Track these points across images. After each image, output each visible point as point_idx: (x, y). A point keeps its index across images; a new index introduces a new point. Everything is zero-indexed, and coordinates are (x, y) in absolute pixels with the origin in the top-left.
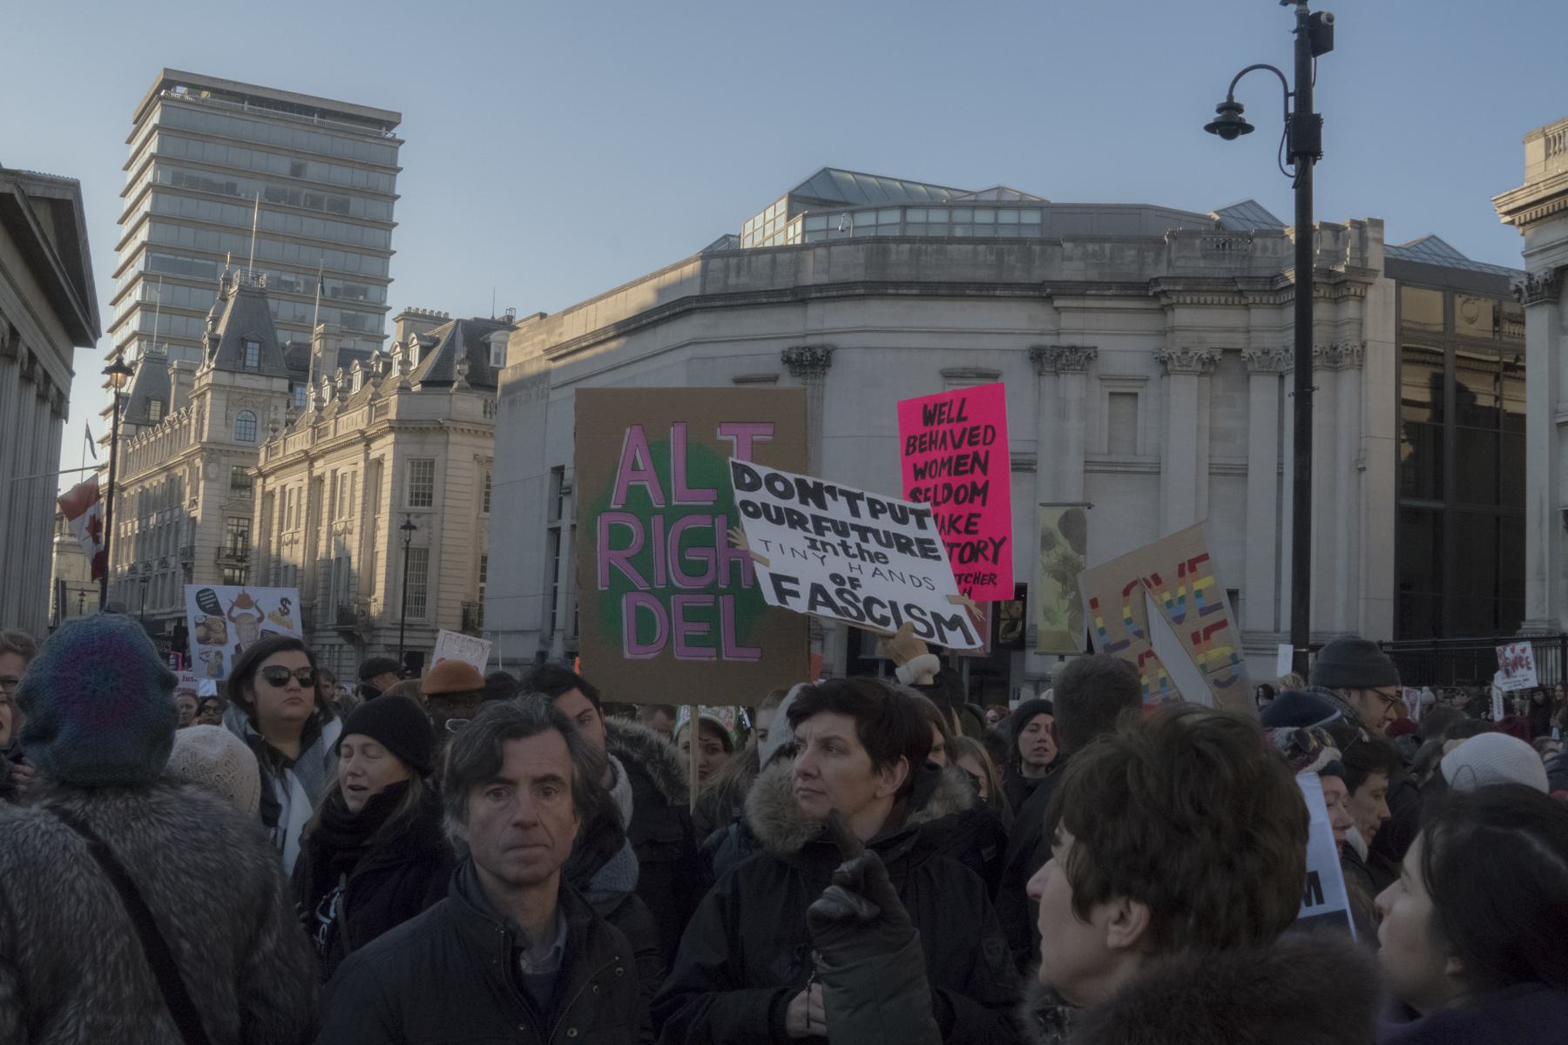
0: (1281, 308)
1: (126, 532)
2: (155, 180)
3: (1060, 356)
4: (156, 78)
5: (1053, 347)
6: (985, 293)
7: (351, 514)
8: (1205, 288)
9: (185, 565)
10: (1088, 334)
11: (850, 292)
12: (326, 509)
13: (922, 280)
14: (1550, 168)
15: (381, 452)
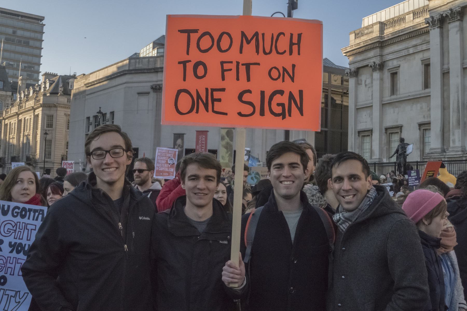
7: (30, 130)
12: (22, 129)
14: (356, 41)
15: (38, 113)
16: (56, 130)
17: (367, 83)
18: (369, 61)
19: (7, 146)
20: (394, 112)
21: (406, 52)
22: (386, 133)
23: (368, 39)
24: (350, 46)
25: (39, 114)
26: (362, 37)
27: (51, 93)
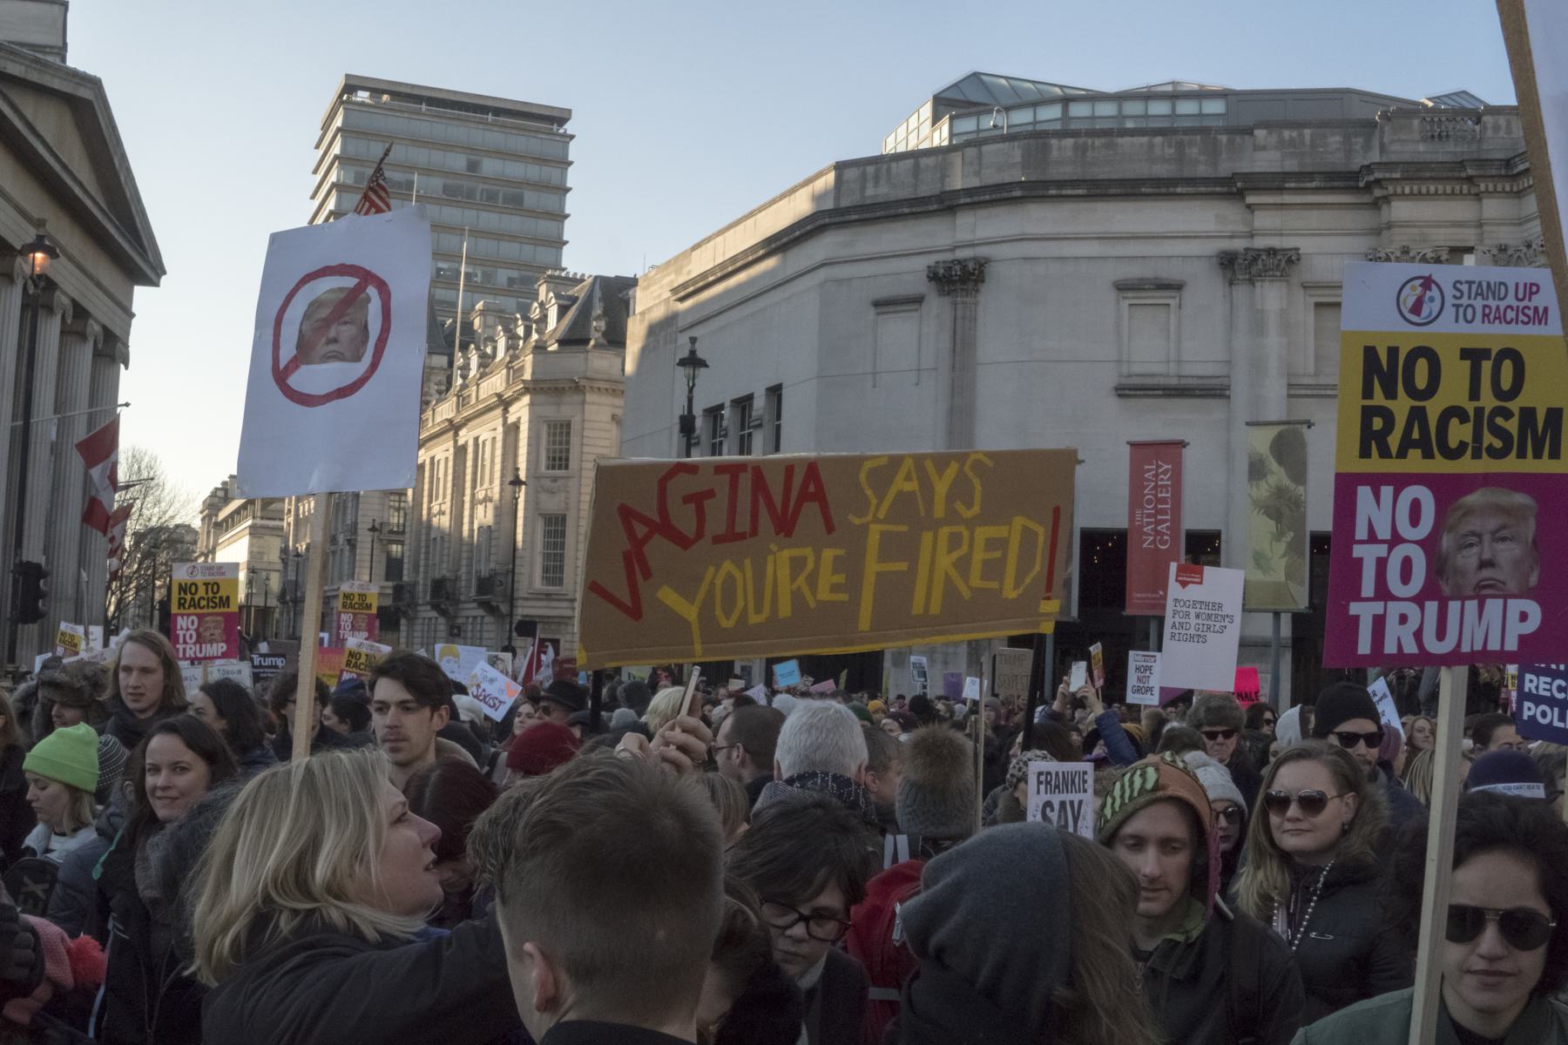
0: (1520, 198)
1: (304, 513)
2: (338, 180)
3: (1255, 259)
4: (340, 83)
5: (1247, 249)
6: (1163, 190)
7: (491, 482)
8: (1428, 175)
9: (349, 541)
10: (1289, 235)
11: (1005, 195)
12: (469, 478)
13: (1089, 178)
15: (518, 415)
16: (581, 477)
19: (423, 544)
25: (519, 418)
27: (561, 342)
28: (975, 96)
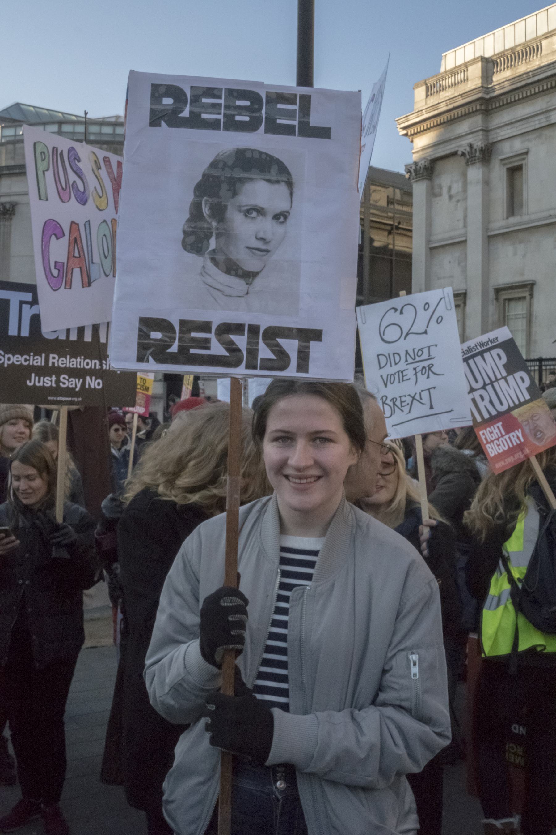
14: (428, 102)
17: (453, 192)
18: (458, 144)
20: (515, 254)
21: (542, 121)
22: (497, 299)
23: (456, 94)
24: (415, 112)
26: (442, 93)
28: (16, 116)
